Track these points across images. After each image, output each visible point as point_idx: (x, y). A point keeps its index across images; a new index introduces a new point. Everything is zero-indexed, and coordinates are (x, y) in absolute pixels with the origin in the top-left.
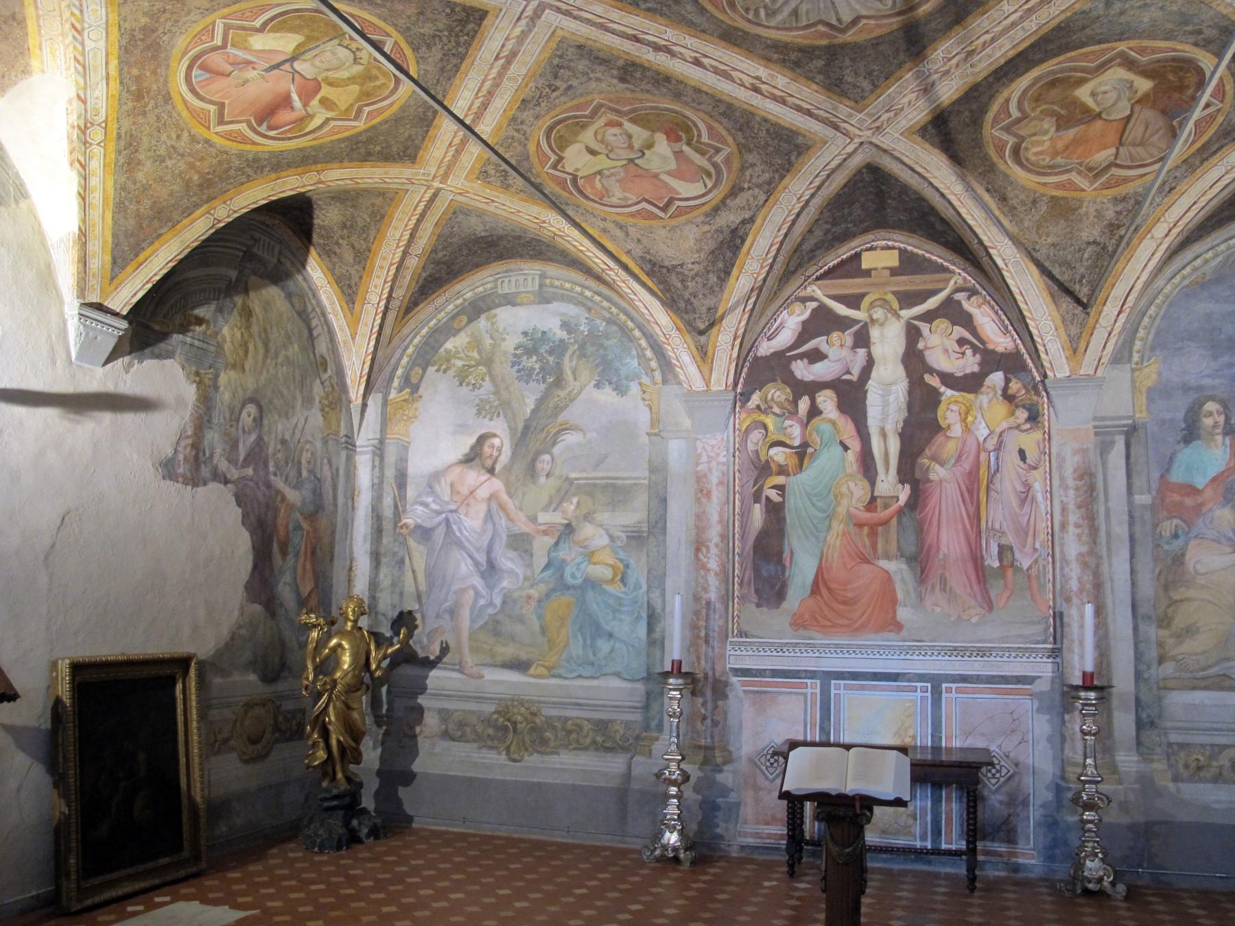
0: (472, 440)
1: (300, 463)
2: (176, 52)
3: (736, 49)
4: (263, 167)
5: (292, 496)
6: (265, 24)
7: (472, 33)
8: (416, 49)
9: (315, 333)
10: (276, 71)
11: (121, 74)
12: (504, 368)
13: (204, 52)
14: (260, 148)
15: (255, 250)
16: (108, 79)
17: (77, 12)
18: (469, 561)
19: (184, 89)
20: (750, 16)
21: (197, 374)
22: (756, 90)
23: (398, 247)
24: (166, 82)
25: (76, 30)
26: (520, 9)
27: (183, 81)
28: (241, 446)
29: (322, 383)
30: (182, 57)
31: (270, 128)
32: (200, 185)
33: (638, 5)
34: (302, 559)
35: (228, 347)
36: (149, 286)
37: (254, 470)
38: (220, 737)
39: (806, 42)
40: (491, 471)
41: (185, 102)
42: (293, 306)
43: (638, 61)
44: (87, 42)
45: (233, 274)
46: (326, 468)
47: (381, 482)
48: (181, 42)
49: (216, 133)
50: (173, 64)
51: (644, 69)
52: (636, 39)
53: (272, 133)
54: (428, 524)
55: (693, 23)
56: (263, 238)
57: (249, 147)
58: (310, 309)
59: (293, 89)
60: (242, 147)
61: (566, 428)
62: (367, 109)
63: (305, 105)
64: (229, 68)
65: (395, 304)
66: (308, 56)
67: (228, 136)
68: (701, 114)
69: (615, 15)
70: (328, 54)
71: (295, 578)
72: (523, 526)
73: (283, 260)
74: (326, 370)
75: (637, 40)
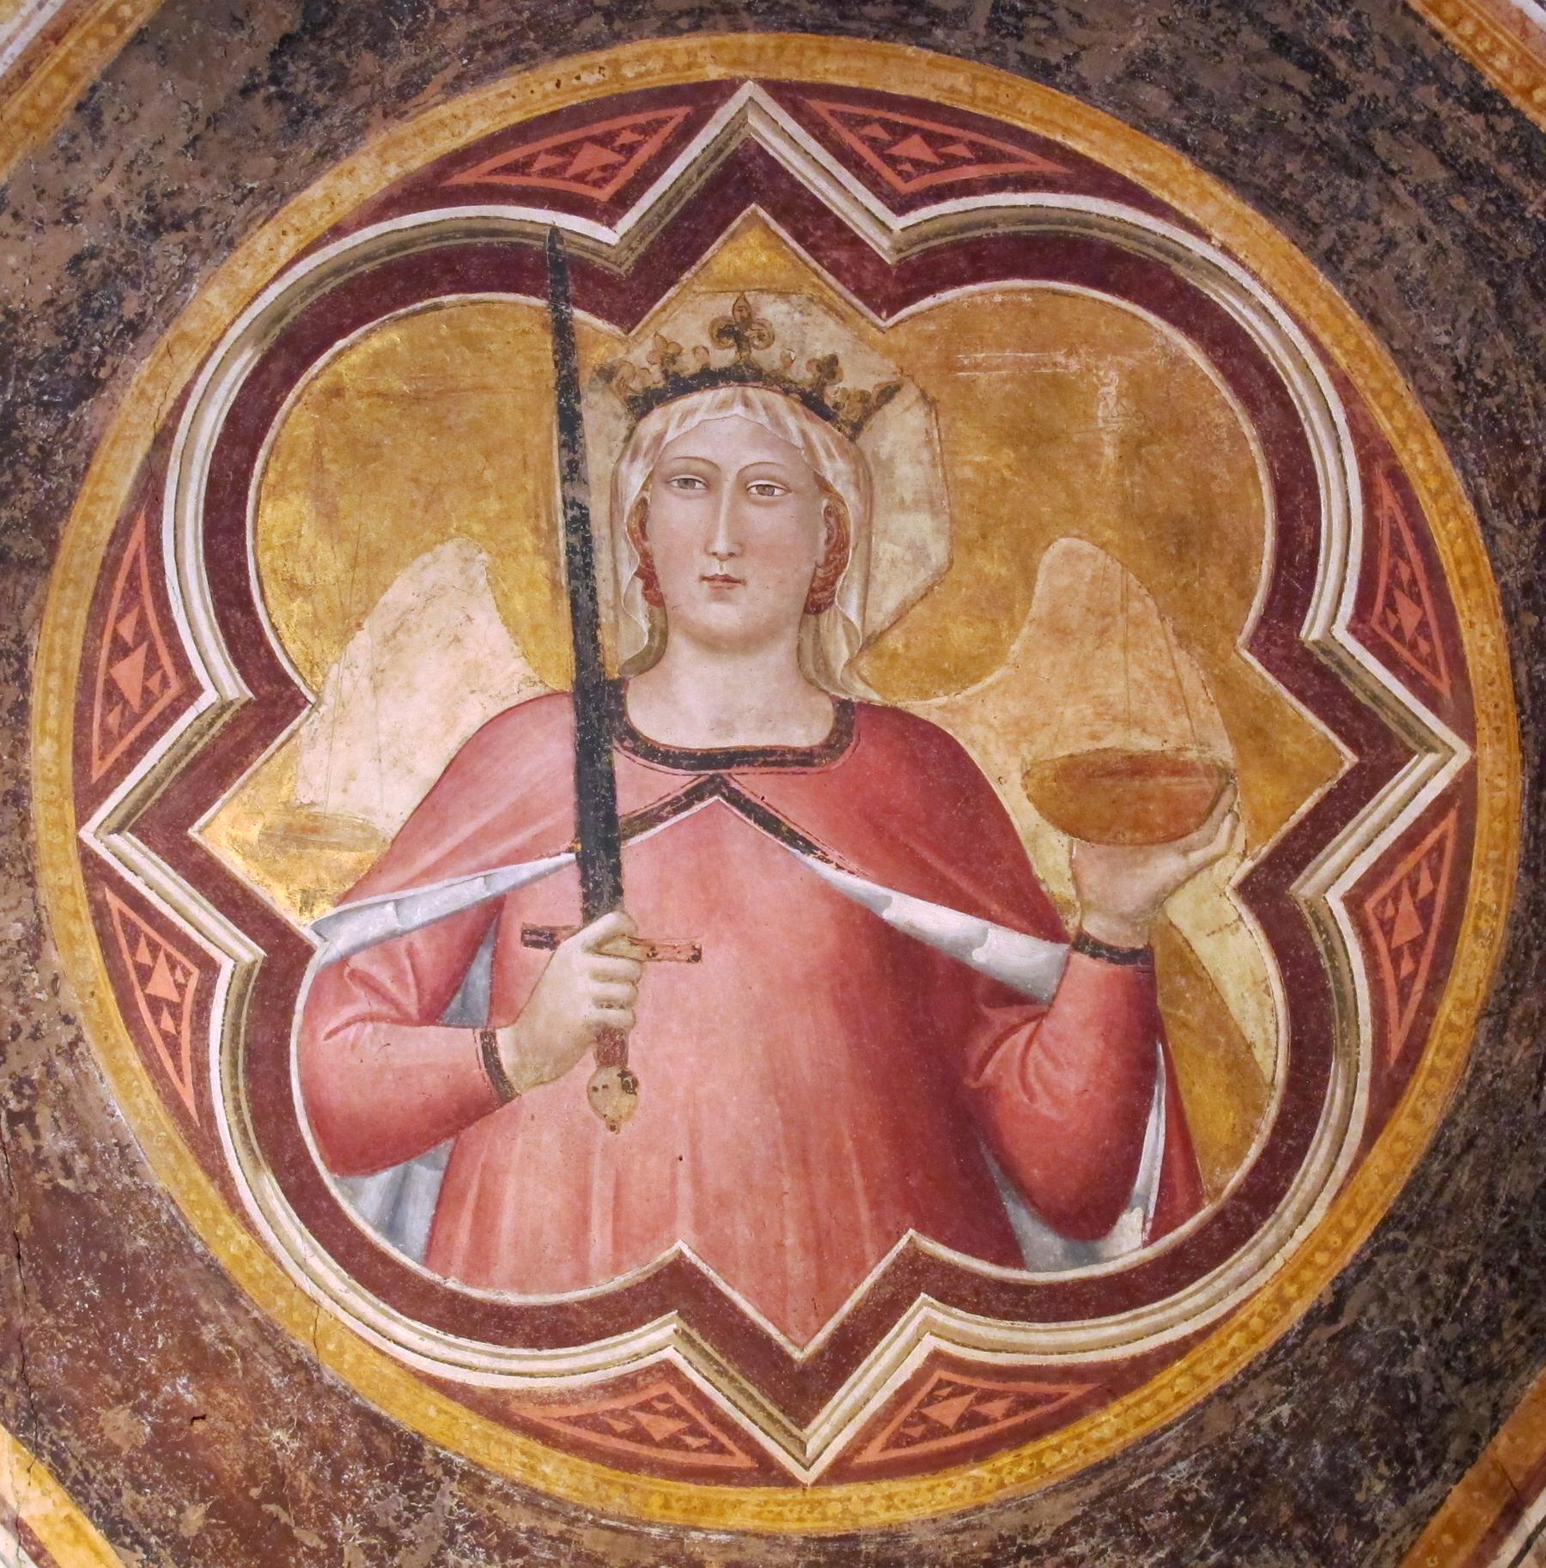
2: (166, 1169)
4: (1338, 1488)
6: (245, 641)
10: (637, 854)
11: (77, 1489)
13: (263, 1064)
14: (1176, 1391)
24: (303, 1371)
27: (365, 1303)
31: (1087, 1220)
41: (494, 1408)
48: (127, 1100)
49: (841, 1471)
50: (226, 1245)
53: (1129, 1243)
57: (1108, 1428)
59: (860, 886)
60: (1064, 1452)
62: (1328, 618)
63: (1037, 914)
64: (445, 1051)
66: (624, 636)
67: (914, 1439)
70: (679, 514)
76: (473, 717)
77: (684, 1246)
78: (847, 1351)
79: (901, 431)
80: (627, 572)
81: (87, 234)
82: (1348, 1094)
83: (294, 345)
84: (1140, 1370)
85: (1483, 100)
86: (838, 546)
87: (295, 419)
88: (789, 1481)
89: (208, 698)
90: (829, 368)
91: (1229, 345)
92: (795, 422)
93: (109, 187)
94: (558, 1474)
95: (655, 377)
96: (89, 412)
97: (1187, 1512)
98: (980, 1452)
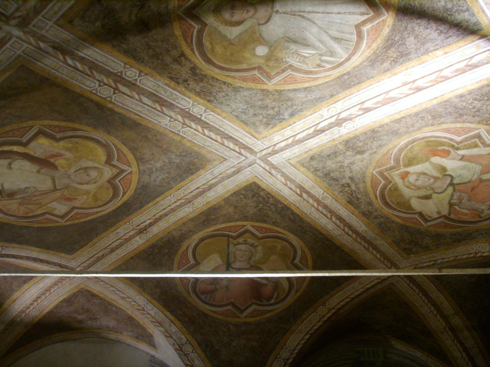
3: (363, 85)
7: (269, 196)
8: (265, 222)
11: (176, 317)
16: (172, 322)
17: (134, 303)
19: (207, 307)
20: (328, 66)
22: (419, 89)
23: (436, 316)
25: (142, 310)
26: (262, 169)
30: (190, 295)
31: (269, 299)
33: (284, 119)
39: (379, 41)
41: (214, 312)
43: (345, 138)
44: (150, 312)
49: (245, 317)
51: (356, 137)
52: (322, 131)
53: (273, 301)
55: (319, 98)
66: (232, 259)
67: (251, 315)
68: (426, 129)
69: (288, 132)
70: (238, 252)
75: (322, 131)
76: (217, 265)
77: (233, 300)
78: (247, 308)
79: (260, 248)
80: (232, 256)
81: (182, 232)
82: (293, 292)
83: (202, 240)
84: (272, 310)
85: (317, 230)
86: (252, 255)
87: (202, 244)
88: (240, 318)
89: (192, 263)
90: (253, 244)
91: (291, 244)
92: (250, 247)
93: (186, 229)
94: (220, 317)
95: (237, 243)
96: (182, 243)
98: (257, 316)
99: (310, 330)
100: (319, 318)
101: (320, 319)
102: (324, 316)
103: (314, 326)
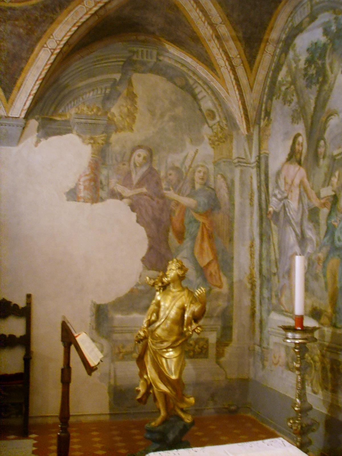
0: (290, 143)
1: (193, 180)
5: (186, 201)
9: (200, 96)
12: (301, 82)
15: (135, 58)
18: (294, 234)
21: (92, 138)
23: (204, 23)
28: (134, 176)
29: (211, 127)
32: (27, 34)
34: (198, 242)
35: (117, 119)
36: (31, 97)
37: (147, 189)
38: (124, 350)
40: (299, 163)
42: (175, 84)
45: (117, 76)
46: (220, 181)
47: (260, 185)
54: (277, 210)
56: (140, 49)
58: (191, 82)
61: (330, 115)
65: (237, 62)
71: (193, 254)
72: (316, 202)
73: (161, 58)
74: (214, 118)
97: (41, 9)
99: (77, 22)
100: (85, 11)
101: (87, 12)
102: (90, 9)
103: (81, 18)
